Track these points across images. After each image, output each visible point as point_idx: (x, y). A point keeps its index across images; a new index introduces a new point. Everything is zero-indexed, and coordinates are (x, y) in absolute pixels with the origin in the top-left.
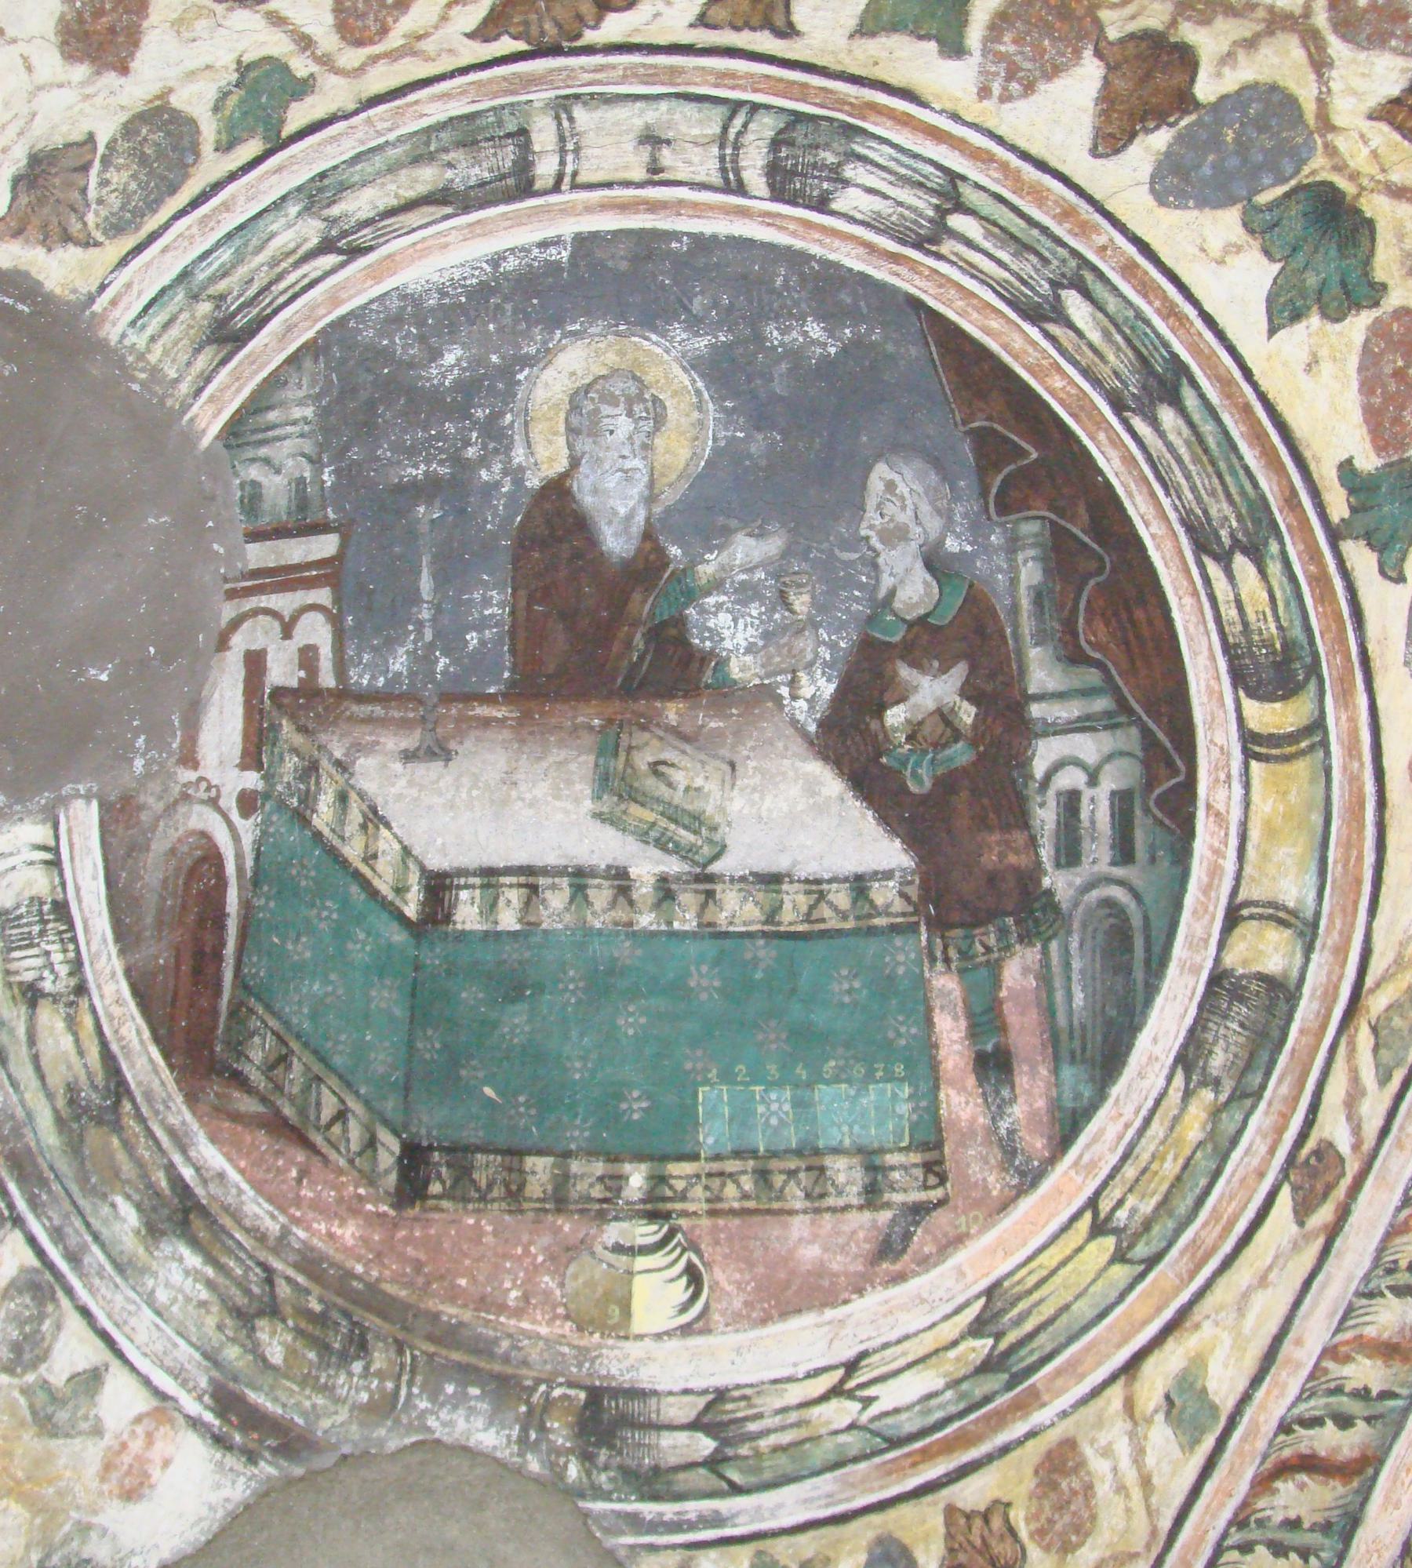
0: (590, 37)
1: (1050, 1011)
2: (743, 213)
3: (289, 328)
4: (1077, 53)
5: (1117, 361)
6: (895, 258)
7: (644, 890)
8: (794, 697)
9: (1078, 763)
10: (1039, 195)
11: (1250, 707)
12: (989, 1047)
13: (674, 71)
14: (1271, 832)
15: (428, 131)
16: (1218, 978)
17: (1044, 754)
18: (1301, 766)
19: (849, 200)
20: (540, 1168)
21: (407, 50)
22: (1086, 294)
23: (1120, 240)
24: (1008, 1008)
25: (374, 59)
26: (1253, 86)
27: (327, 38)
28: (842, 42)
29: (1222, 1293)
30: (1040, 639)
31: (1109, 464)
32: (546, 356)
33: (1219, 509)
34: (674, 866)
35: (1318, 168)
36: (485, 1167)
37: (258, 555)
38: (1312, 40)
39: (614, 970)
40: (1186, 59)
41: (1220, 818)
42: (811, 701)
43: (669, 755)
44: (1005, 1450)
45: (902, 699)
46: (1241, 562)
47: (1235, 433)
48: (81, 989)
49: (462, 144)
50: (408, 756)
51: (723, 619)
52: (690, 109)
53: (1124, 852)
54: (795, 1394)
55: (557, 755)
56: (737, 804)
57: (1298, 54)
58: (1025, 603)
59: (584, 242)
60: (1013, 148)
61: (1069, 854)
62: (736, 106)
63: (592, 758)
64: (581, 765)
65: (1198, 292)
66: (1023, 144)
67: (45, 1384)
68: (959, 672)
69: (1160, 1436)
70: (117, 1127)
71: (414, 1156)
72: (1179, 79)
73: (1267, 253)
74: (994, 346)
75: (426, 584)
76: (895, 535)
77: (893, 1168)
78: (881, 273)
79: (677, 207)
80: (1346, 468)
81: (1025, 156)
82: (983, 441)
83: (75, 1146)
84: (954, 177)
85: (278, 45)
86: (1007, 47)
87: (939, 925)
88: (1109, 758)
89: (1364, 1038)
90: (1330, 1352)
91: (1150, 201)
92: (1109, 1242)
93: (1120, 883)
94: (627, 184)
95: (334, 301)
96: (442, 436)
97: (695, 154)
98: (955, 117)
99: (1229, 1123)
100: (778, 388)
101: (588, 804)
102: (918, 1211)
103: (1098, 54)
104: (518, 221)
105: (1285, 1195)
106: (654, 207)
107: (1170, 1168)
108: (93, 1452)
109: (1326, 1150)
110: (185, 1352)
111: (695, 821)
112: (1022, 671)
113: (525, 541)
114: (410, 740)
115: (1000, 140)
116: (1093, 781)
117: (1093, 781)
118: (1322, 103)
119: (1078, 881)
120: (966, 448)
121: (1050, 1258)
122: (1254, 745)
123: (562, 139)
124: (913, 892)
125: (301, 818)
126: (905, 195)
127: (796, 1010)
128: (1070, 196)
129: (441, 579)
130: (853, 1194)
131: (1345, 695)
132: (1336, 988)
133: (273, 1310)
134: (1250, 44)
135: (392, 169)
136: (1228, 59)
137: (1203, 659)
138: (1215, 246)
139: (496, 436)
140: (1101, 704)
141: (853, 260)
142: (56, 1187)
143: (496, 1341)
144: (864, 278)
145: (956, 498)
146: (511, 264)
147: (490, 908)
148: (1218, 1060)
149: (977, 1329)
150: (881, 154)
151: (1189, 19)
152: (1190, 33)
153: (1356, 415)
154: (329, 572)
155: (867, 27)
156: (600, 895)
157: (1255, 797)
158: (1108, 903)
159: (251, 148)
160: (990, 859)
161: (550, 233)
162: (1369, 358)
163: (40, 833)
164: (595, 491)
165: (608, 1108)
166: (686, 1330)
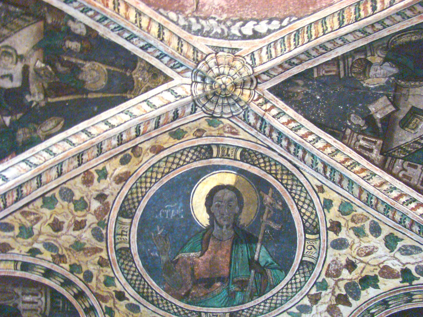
5: (381, 307)
22: (371, 310)
31: (396, 311)
33: (405, 298)
35: (357, 281)
38: (339, 280)
40: (340, 295)
46: (413, 297)
57: (341, 282)
73: (368, 288)
80: (401, 282)
118: (348, 280)
134: (339, 287)
136: (340, 290)
138: (366, 294)
153: (393, 280)
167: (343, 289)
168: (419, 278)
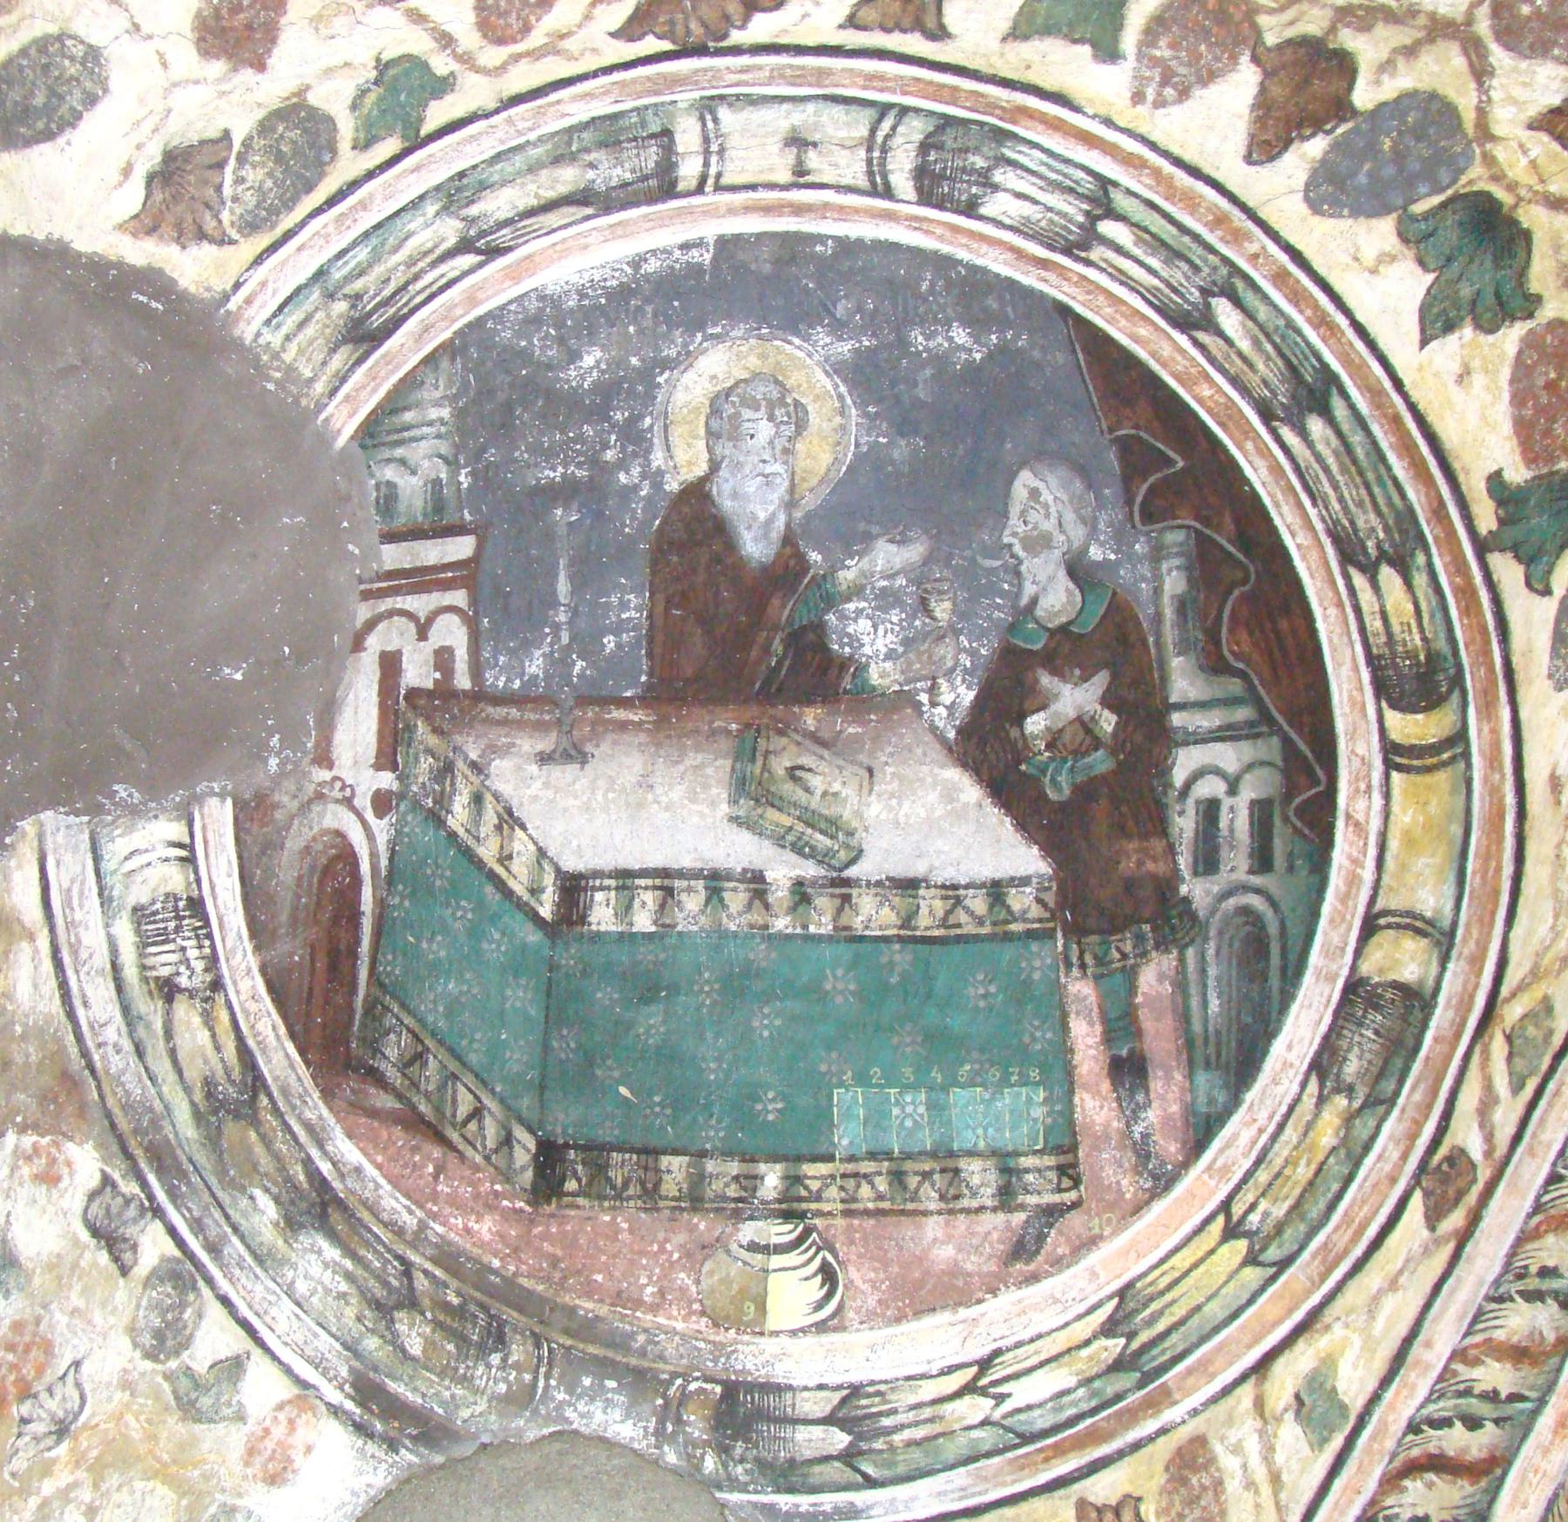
0: (736, 37)
1: (1185, 1018)
2: (890, 216)
3: (426, 329)
4: (1234, 59)
5: (1267, 370)
6: (1043, 264)
7: (780, 893)
8: (934, 704)
9: (1218, 772)
10: (1191, 202)
11: (1393, 718)
12: (1124, 1053)
13: (821, 75)
14: (1409, 841)
15: (570, 131)
16: (1354, 986)
17: (1185, 762)
18: (1442, 778)
19: (995, 205)
20: (675, 1168)
21: (550, 49)
22: (1237, 303)
23: (1273, 248)
24: (1144, 1015)
25: (516, 58)
26: (1411, 95)
27: (468, 36)
28: (995, 45)
29: (1354, 1295)
30: (1183, 648)
31: (1256, 474)
32: (686, 359)
33: (1366, 520)
34: (810, 870)
35: (1475, 177)
36: (621, 1167)
37: (394, 556)
39: (749, 971)
40: (1345, 65)
41: (1359, 828)
42: (951, 708)
43: (806, 760)
44: (1137, 1446)
45: (1043, 708)
46: (1387, 574)
47: (1384, 445)
48: (217, 985)
49: (602, 145)
50: (544, 759)
51: (864, 625)
52: (837, 111)
53: (1262, 860)
54: (929, 1390)
55: (693, 759)
56: (875, 809)
57: (1459, 62)
58: (1169, 613)
59: (726, 245)
60: (1166, 154)
61: (1207, 862)
62: (884, 109)
63: (728, 763)
64: (718, 768)
65: (1351, 302)
66: (1176, 150)
67: (188, 1371)
68: (1101, 680)
69: (1290, 1434)
70: (255, 1122)
71: (549, 1155)
72: (1336, 86)
73: (1422, 263)
74: (1142, 354)
75: (563, 587)
76: (1038, 543)
77: (1027, 1171)
78: (1029, 278)
79: (823, 210)
80: (1495, 480)
81: (1178, 162)
82: (1126, 447)
83: (213, 1139)
84: (1105, 183)
85: (418, 43)
86: (1162, 51)
87: (1076, 931)
88: (1250, 767)
89: (1498, 1047)
90: (1459, 1355)
91: (1303, 209)
92: (1241, 1245)
93: (1258, 891)
94: (772, 186)
95: (472, 301)
96: (580, 439)
97: (842, 157)
98: (1108, 122)
99: (1362, 1129)
100: (921, 393)
101: (724, 808)
102: (1052, 1213)
103: (1255, 59)
104: (661, 222)
105: (1417, 1200)
106: (799, 210)
107: (1303, 1172)
108: (235, 1438)
109: (1458, 1157)
110: (325, 1343)
111: (832, 826)
112: (1164, 679)
113: (663, 546)
114: (545, 743)
115: (1153, 146)
116: (1233, 790)
117: (1233, 790)
118: (1482, 113)
119: (1216, 889)
120: (1112, 457)
121: (1182, 1261)
122: (1395, 755)
123: (706, 140)
124: (1050, 898)
125: (436, 818)
126: (1054, 200)
127: (931, 1015)
128: (1223, 203)
129: (579, 584)
130: (987, 1197)
131: (1488, 708)
132: (1472, 997)
133: (411, 1302)
134: (1410, 51)
135: (532, 169)
136: (1386, 67)
137: (1346, 670)
138: (1369, 255)
139: (635, 439)
140: (1243, 714)
141: (999, 265)
142: (195, 1179)
143: (632, 1336)
144: (1011, 283)
145: (1100, 506)
146: (652, 266)
147: (625, 910)
148: (1352, 1067)
149: (1109, 1328)
150: (1031, 159)
151: (1348, 25)
152: (1349, 40)
153: (1507, 427)
154: (465, 574)
155: (1019, 31)
156: (736, 899)
157: (1396, 808)
158: (1245, 911)
159: (389, 147)
160: (1128, 865)
161: (692, 234)
162: (1522, 370)
163: (177, 831)
164: (735, 495)
165: (743, 1107)
166: (821, 1327)
167: (1403, 81)
168: (1547, 592)
